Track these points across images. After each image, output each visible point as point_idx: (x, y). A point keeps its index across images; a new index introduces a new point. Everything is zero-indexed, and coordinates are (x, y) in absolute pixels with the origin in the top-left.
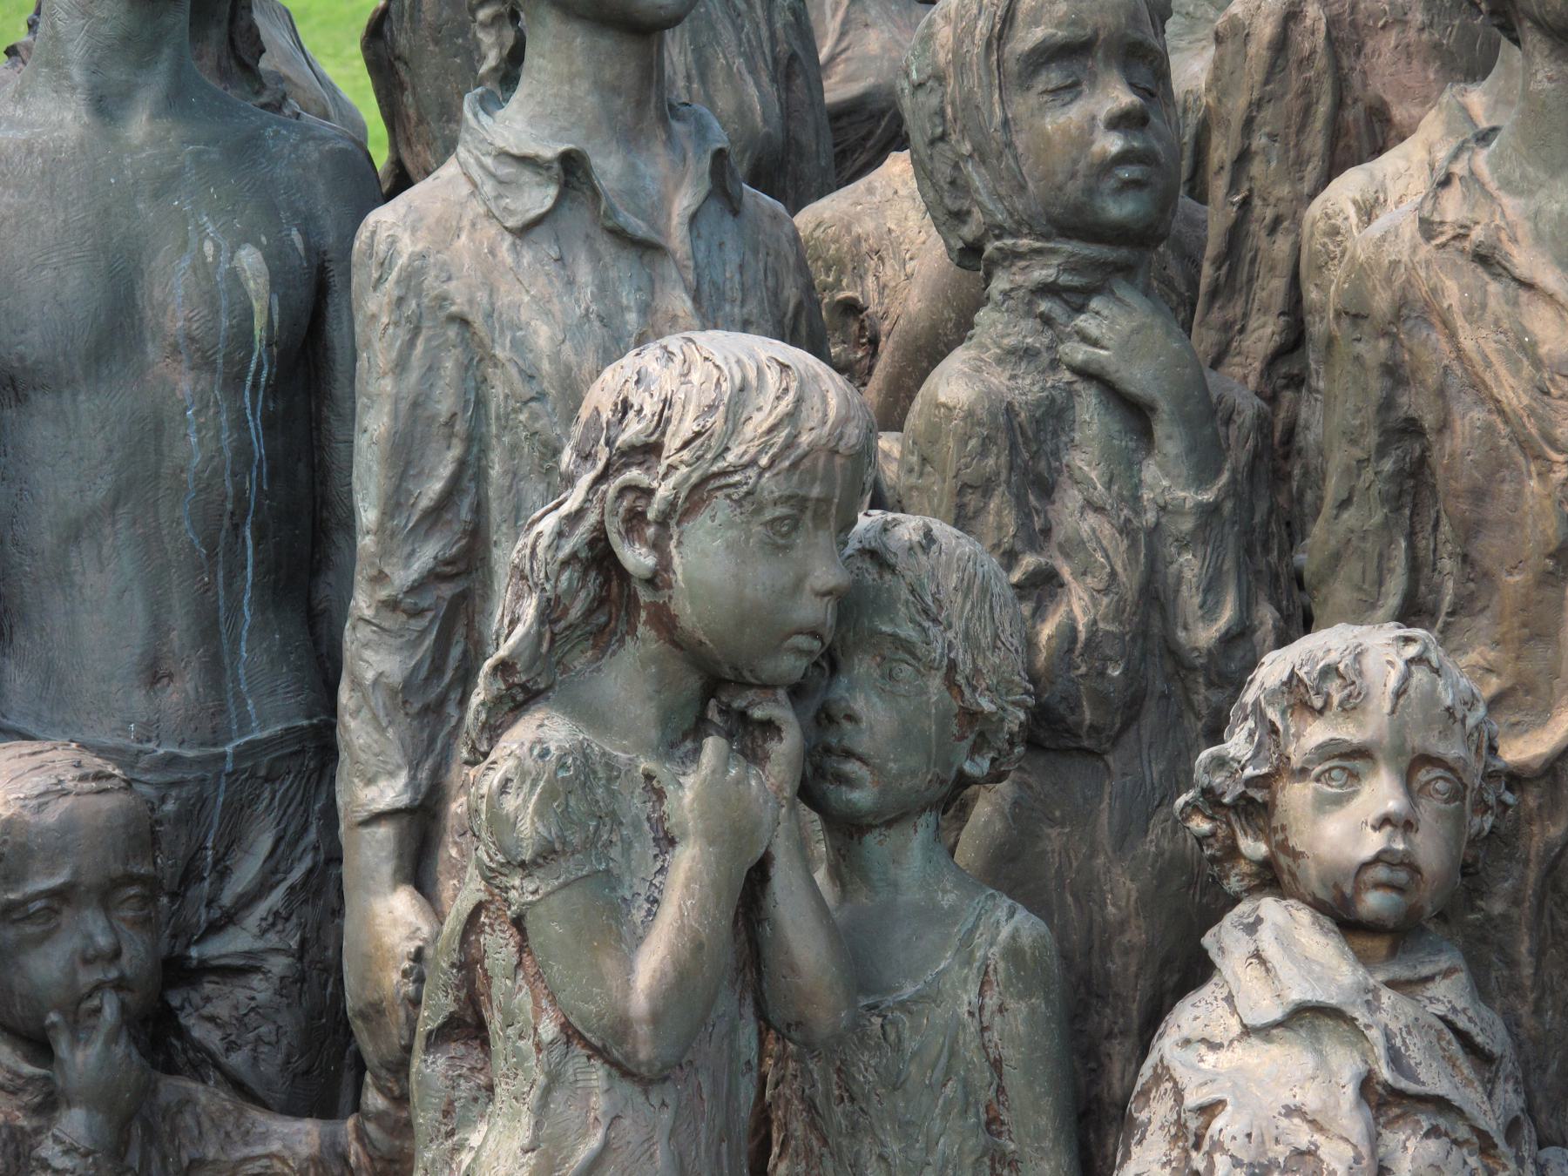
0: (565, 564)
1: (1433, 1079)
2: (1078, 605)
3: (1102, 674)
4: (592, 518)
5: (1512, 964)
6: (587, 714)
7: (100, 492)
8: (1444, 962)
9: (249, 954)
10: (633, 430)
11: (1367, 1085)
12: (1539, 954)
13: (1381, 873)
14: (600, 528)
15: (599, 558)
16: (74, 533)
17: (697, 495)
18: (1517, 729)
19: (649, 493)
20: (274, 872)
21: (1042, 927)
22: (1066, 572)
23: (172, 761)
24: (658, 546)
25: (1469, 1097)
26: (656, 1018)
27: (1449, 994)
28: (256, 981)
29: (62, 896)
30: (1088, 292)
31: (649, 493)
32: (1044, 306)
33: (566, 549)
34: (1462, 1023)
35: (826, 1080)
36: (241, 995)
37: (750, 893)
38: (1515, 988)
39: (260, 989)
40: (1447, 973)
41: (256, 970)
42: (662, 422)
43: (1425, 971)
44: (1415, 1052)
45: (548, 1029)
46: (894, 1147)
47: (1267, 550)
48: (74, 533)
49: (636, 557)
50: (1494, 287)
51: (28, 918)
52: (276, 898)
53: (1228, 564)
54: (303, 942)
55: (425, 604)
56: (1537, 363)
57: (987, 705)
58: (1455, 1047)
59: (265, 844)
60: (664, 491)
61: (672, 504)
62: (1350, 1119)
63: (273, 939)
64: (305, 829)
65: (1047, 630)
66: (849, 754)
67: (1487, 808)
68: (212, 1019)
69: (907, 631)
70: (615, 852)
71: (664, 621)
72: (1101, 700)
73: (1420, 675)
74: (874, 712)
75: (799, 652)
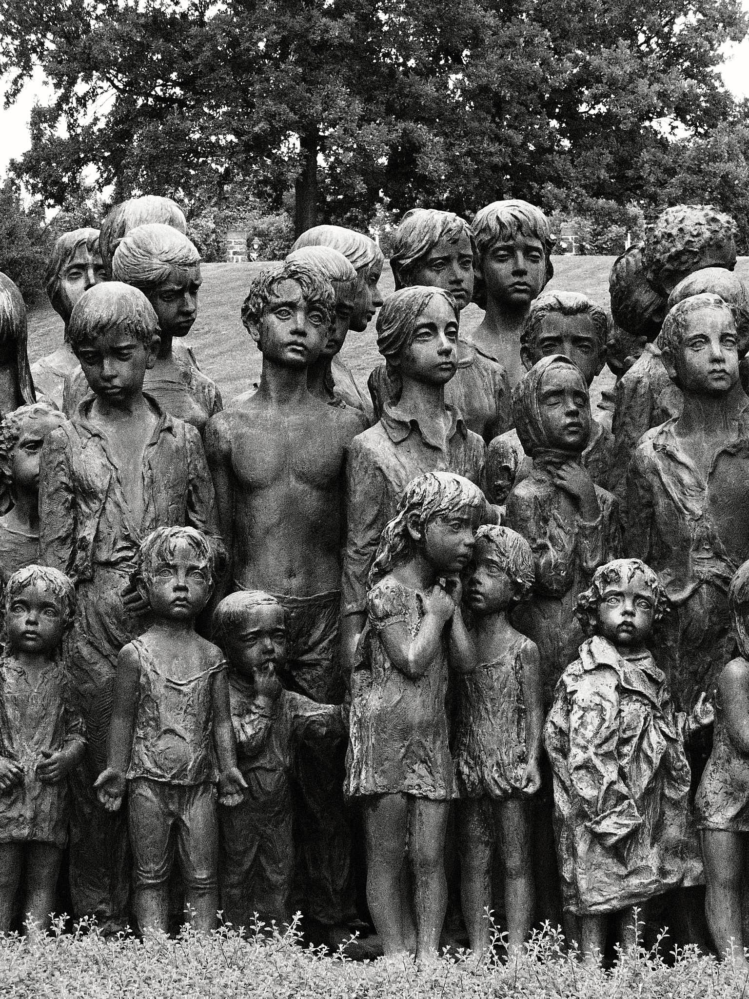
0: (395, 536)
1: (638, 686)
2: (553, 554)
3: (559, 574)
4: (403, 523)
5: (674, 660)
6: (403, 580)
7: (275, 519)
8: (645, 655)
9: (316, 660)
10: (416, 499)
11: (619, 689)
12: (681, 658)
13: (624, 627)
14: (406, 526)
15: (405, 535)
16: (268, 531)
17: (433, 517)
18: (675, 591)
19: (419, 516)
20: (325, 635)
21: (535, 644)
22: (550, 545)
23: (295, 600)
24: (421, 532)
25: (649, 692)
26: (416, 662)
27: (647, 663)
28: (319, 668)
29: (259, 635)
30: (562, 463)
31: (419, 516)
32: (549, 468)
33: (396, 531)
34: (649, 672)
35: (471, 687)
36: (314, 672)
37: (446, 631)
38: (674, 667)
39: (320, 671)
40: (645, 658)
41: (319, 664)
42: (423, 497)
43: (639, 657)
44: (633, 678)
45: (387, 665)
46: (489, 706)
47: (614, 541)
48: (268, 531)
49: (416, 535)
50: (672, 464)
51: (249, 640)
52: (324, 644)
53: (600, 544)
54: (333, 657)
55: (366, 552)
56: (682, 485)
57: (519, 580)
58: (646, 679)
59: (323, 626)
60: (423, 516)
61: (425, 519)
62: (613, 696)
63: (323, 655)
64: (334, 623)
65: (543, 561)
66: (478, 593)
67: (660, 612)
68: (305, 679)
69: (496, 559)
70: (407, 616)
71: (424, 553)
72: (558, 582)
73: (638, 572)
74: (488, 583)
75: (460, 562)
